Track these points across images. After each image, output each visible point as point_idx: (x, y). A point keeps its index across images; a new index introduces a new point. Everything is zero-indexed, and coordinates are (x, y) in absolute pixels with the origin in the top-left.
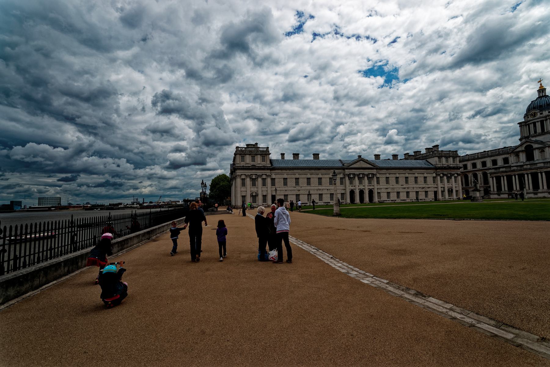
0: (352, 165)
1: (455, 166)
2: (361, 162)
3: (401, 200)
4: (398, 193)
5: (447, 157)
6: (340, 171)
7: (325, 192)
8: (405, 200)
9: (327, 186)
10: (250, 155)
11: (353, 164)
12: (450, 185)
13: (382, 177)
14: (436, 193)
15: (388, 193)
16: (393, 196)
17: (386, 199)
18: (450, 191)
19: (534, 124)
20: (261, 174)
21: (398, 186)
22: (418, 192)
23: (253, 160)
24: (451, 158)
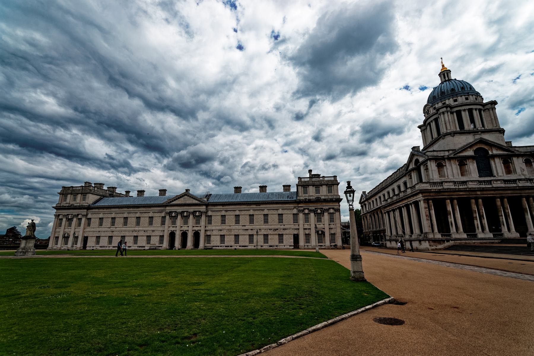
0: (173, 201)
1: (330, 197)
2: (186, 197)
3: (240, 246)
4: (237, 236)
5: (317, 186)
6: (162, 208)
7: (142, 233)
8: (246, 246)
9: (144, 226)
10: (71, 194)
11: (175, 200)
12: (322, 226)
13: (215, 216)
14: (296, 238)
15: (222, 237)
16: (230, 241)
17: (219, 244)
18: (321, 235)
19: (429, 124)
20: (76, 214)
21: (237, 227)
22: (268, 235)
23: (75, 199)
24: (324, 187)
